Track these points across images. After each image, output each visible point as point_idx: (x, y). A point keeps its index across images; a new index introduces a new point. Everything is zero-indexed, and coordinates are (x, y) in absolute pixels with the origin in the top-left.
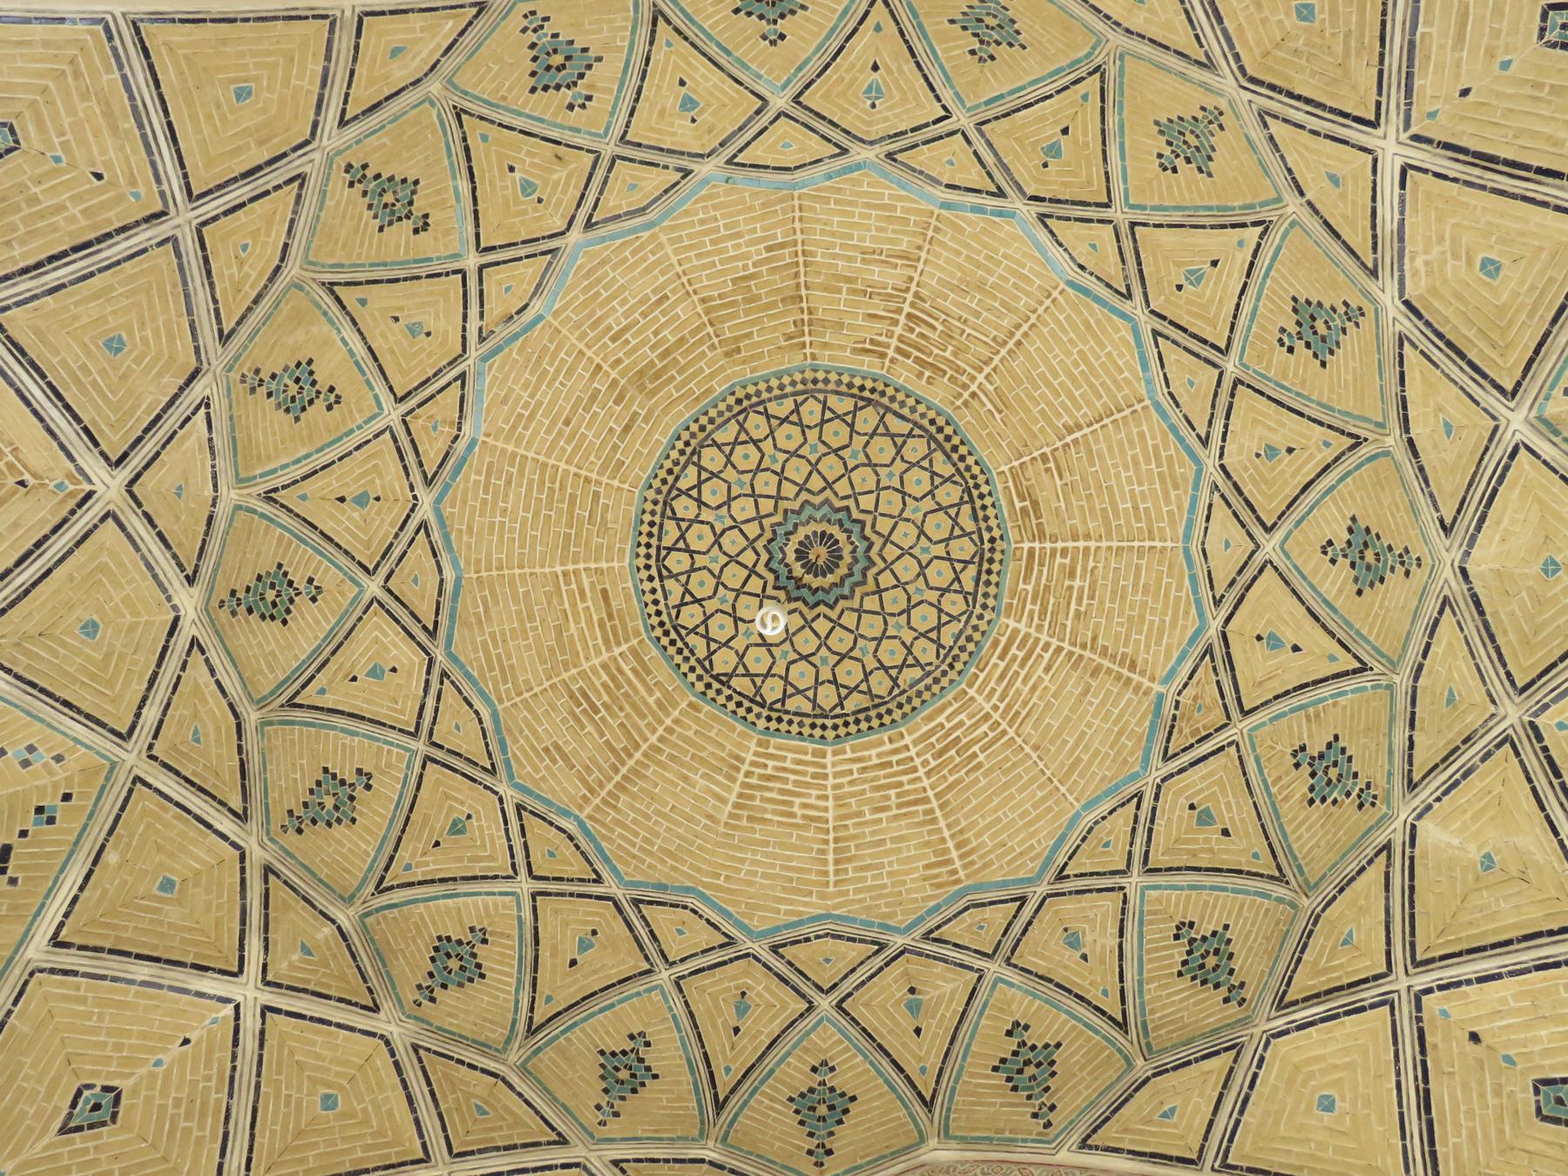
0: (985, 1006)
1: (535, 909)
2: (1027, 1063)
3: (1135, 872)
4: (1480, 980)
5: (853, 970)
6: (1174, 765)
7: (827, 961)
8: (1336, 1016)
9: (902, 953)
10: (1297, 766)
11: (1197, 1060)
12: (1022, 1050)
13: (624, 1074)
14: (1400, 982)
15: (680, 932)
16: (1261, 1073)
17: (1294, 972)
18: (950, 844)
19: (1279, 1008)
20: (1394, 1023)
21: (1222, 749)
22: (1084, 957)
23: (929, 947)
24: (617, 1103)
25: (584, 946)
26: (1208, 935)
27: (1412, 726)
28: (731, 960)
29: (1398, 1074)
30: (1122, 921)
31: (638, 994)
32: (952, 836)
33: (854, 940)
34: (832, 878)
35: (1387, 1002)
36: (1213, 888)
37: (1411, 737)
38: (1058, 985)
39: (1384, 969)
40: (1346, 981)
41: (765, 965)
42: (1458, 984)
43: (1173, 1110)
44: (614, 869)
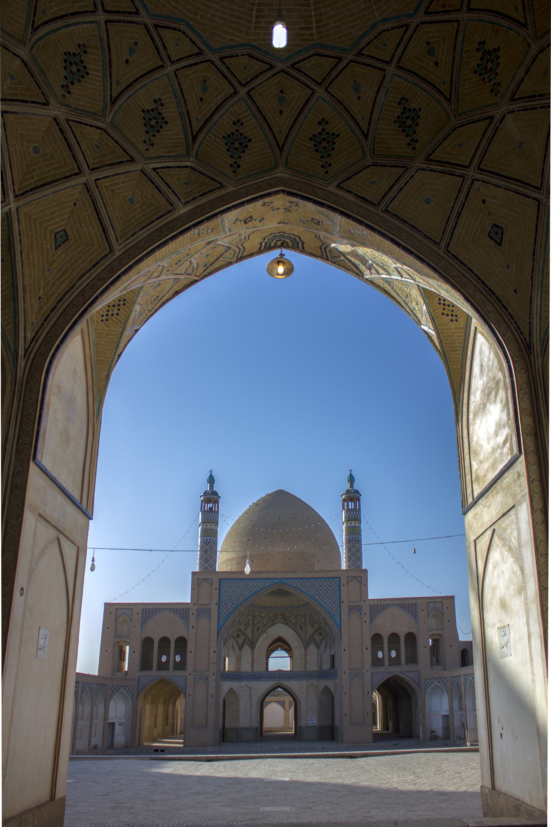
0: (312, 108)
1: (107, 30)
2: (324, 139)
3: (393, 66)
4: (495, 185)
5: (257, 77)
6: (428, 18)
7: (245, 68)
8: (445, 173)
9: (280, 72)
10: (478, 50)
11: (390, 166)
12: (323, 133)
13: (153, 122)
14: (471, 173)
15: (177, 45)
16: (410, 181)
17: (437, 147)
18: (314, 19)
19: (426, 160)
20: (462, 185)
21: (451, 21)
22: (359, 98)
23: (292, 72)
24: (152, 138)
25: (132, 52)
26: (412, 109)
27: (526, 74)
28: (201, 62)
29: (455, 203)
30: (380, 86)
31: (157, 78)
32: (316, 15)
33: (258, 60)
34: (253, 25)
35: (463, 177)
36: (422, 88)
37: (523, 78)
38: (345, 108)
39: (467, 164)
40: (453, 162)
41: (216, 67)
42: (488, 183)
43: (374, 182)
44: (145, 6)
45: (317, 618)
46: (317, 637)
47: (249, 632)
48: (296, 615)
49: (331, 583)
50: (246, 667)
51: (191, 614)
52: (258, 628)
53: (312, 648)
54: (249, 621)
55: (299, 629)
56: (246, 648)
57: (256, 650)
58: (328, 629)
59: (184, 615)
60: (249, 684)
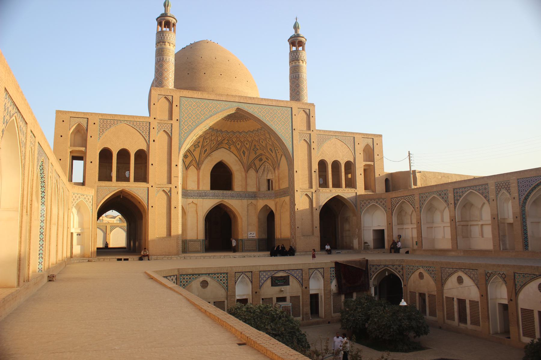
45: (264, 144)
46: (257, 163)
47: (196, 154)
48: (242, 140)
49: (284, 112)
50: (192, 186)
51: (151, 128)
52: (206, 151)
53: (252, 172)
54: (199, 143)
55: (242, 154)
56: (192, 169)
57: (201, 171)
58: (273, 154)
59: (145, 129)
60: (195, 201)
